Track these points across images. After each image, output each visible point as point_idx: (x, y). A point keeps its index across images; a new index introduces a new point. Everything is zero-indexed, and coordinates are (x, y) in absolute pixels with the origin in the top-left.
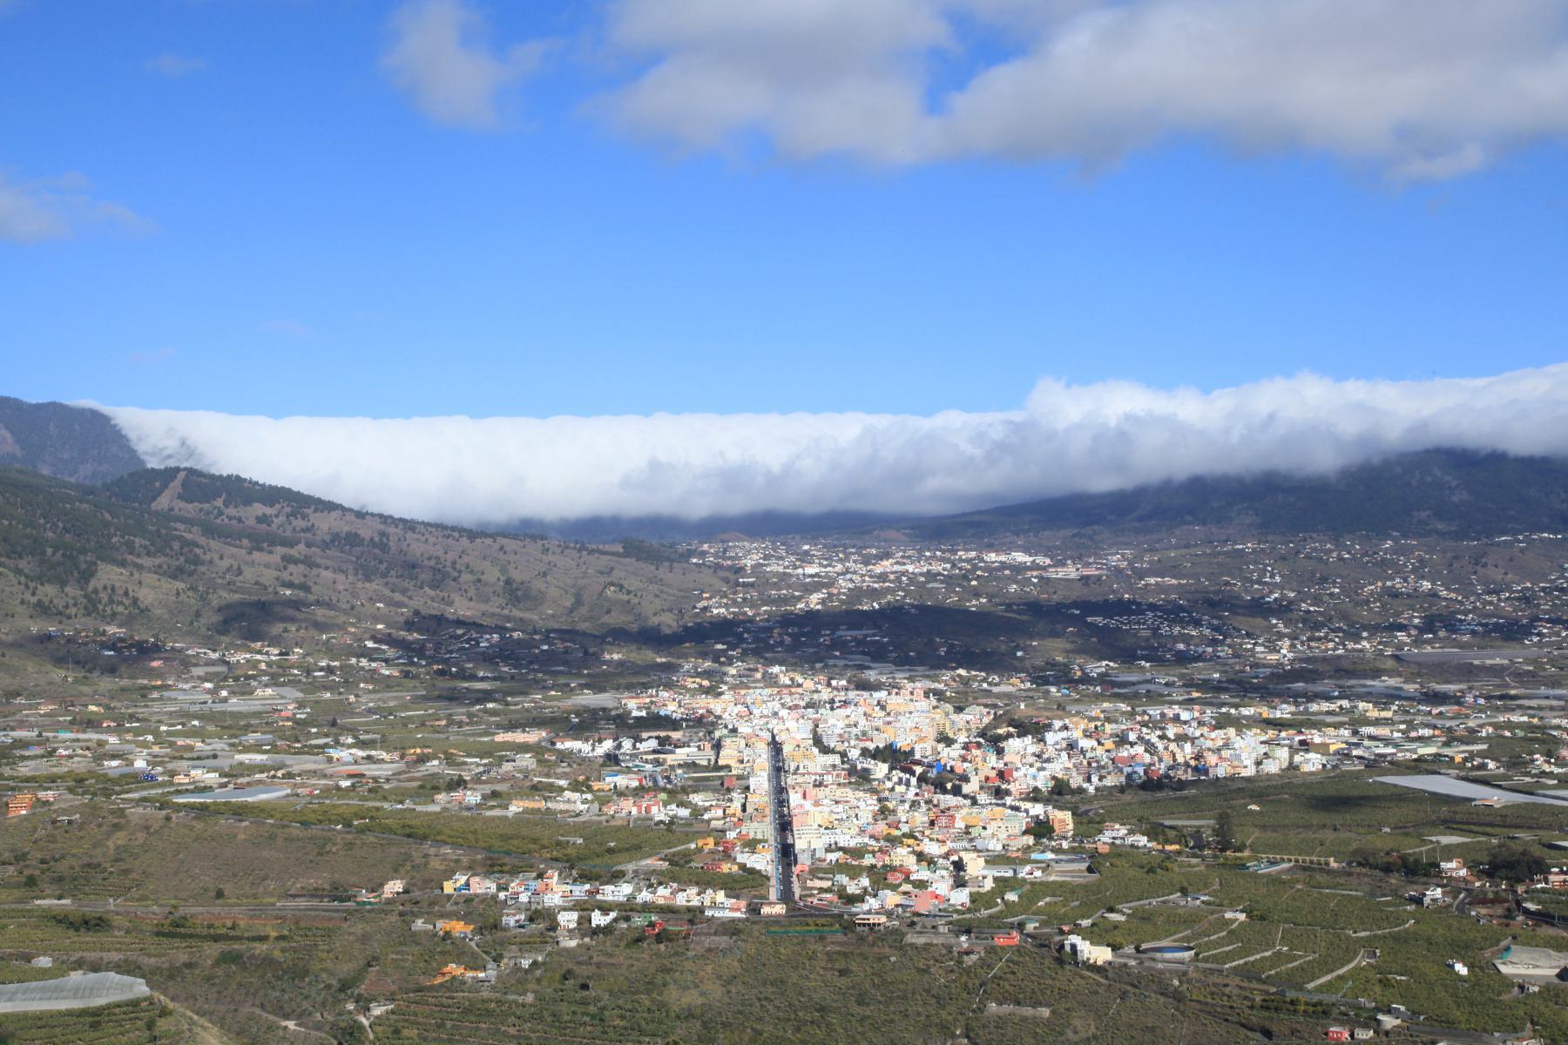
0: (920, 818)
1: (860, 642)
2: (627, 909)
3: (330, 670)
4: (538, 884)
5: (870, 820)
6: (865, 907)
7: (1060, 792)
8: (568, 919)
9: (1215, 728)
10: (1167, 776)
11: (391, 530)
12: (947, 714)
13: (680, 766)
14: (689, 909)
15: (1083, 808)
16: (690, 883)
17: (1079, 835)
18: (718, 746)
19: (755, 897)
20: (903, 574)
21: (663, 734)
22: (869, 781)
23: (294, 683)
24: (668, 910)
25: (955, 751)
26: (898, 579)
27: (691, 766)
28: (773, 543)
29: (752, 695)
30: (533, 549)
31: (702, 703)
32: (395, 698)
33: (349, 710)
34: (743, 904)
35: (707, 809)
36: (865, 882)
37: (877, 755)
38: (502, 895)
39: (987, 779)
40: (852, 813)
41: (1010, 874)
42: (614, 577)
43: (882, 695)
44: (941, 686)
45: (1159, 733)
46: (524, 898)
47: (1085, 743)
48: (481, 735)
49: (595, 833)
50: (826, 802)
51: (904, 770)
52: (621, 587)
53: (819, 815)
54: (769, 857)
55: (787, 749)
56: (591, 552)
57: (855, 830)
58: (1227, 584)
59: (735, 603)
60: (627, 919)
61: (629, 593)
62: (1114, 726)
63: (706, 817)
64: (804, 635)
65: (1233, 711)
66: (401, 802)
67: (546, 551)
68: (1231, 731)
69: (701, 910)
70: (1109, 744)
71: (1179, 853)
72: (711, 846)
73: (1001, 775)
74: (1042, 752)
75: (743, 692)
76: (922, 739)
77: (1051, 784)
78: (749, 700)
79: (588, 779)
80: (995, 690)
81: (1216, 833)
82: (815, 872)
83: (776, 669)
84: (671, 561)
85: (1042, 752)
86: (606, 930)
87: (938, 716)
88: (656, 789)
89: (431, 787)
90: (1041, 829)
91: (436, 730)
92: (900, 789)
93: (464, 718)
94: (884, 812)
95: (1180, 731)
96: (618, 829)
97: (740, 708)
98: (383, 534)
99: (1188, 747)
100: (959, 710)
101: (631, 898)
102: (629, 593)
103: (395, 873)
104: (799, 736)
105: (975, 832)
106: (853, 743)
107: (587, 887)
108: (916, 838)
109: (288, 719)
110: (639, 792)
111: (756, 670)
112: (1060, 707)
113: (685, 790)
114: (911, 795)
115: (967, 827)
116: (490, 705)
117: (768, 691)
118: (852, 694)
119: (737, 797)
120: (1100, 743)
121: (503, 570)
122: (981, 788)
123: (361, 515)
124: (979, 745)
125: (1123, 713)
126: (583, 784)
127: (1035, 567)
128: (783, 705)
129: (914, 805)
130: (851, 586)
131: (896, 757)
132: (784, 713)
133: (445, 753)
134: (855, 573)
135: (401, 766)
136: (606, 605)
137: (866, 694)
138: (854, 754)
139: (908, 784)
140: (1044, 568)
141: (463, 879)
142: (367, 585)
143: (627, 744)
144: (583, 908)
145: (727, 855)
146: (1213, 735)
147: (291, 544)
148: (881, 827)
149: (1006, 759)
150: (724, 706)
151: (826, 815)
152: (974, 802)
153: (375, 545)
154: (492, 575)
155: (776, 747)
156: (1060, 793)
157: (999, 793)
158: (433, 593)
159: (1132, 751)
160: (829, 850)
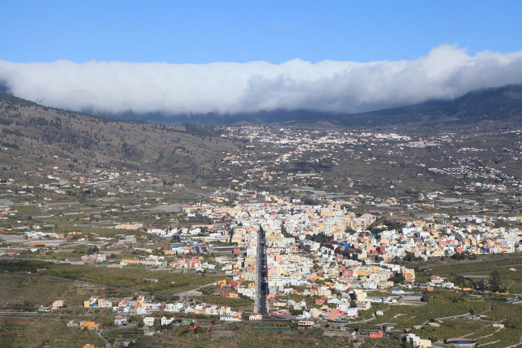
0: (335, 271)
1: (308, 180)
3: (28, 190)
4: (134, 303)
5: (309, 272)
6: (303, 317)
7: (409, 259)
8: (149, 321)
9: (495, 227)
10: (467, 252)
11: (62, 117)
12: (352, 218)
13: (211, 243)
14: (212, 317)
15: (421, 268)
16: (213, 303)
17: (418, 282)
18: (231, 233)
19: (246, 310)
20: (332, 144)
21: (203, 226)
22: (309, 251)
23: (9, 197)
24: (201, 317)
25: (355, 237)
26: (329, 147)
27: (218, 243)
28: (265, 127)
29: (251, 207)
30: (138, 128)
31: (224, 210)
32: (63, 205)
33: (38, 212)
34: (239, 314)
35: (224, 265)
36: (304, 304)
37: (313, 238)
38: (115, 308)
39: (371, 251)
40: (299, 268)
41: (380, 301)
42: (182, 142)
43: (318, 207)
44: (350, 203)
45: (463, 229)
46: (126, 310)
47: (424, 234)
48: (108, 225)
50: (286, 262)
51: (328, 246)
52: (184, 149)
53: (281, 269)
54: (254, 290)
55: (268, 235)
56: (169, 130)
57: (300, 277)
58: (505, 151)
59: (243, 158)
60: (180, 321)
61: (188, 152)
62: (439, 225)
63: (223, 269)
64: (279, 175)
65: (505, 219)
66: (63, 260)
67: (145, 129)
68: (503, 229)
69: (218, 317)
70: (436, 235)
71: (470, 292)
72: (225, 284)
73: (378, 249)
74: (401, 238)
75: (246, 205)
76: (338, 231)
77: (405, 255)
78: (249, 209)
79: (162, 249)
80: (378, 205)
81: (491, 282)
82: (278, 299)
83: (264, 193)
84: (211, 136)
85: (401, 238)
86: (169, 327)
87: (347, 218)
88: (198, 254)
89: (80, 252)
90: (398, 278)
91: (85, 223)
92: (326, 256)
93: (99, 216)
94: (316, 268)
95: (474, 228)
96: (176, 275)
97: (244, 213)
98: (58, 119)
99: (478, 237)
100: (359, 215)
101: (182, 310)
102: (188, 152)
103: (59, 296)
104: (274, 228)
105: (363, 279)
106: (302, 232)
107: (159, 304)
108: (332, 282)
109: (5, 216)
110: (189, 256)
111: (254, 193)
112: (412, 215)
113: (213, 255)
114: (331, 259)
115: (359, 276)
116: (113, 210)
117: (259, 204)
118: (303, 207)
119: (240, 259)
120: (431, 234)
121: (122, 139)
122: (368, 256)
123: (46, 109)
124: (367, 234)
125: (446, 219)
126: (160, 251)
127: (402, 141)
128: (266, 212)
129: (332, 264)
130: (304, 150)
131: (324, 239)
132: (267, 216)
133: (89, 234)
134: (307, 143)
135: (64, 241)
136: (176, 158)
137: (310, 207)
138: (302, 237)
139: (330, 254)
140: (407, 142)
141: (95, 300)
142: (49, 146)
143: (185, 231)
144: (157, 315)
145: (233, 289)
146: (492, 231)
147: (8, 123)
148: (314, 276)
149: (382, 241)
150: (237, 212)
151: (285, 269)
152: (364, 264)
153: (54, 125)
154: (116, 141)
155: (262, 233)
156: (409, 260)
157: (377, 259)
158: (84, 151)
159: (449, 239)
160: (285, 287)
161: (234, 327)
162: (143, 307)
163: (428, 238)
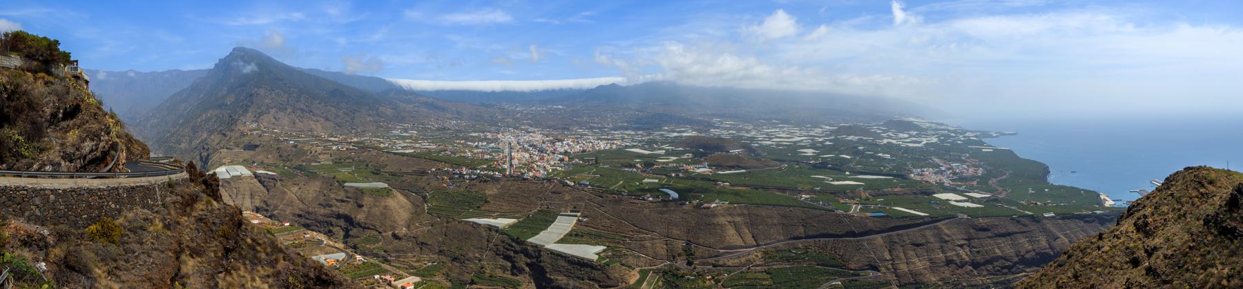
2: (479, 176)
7: (566, 153)
49: (472, 160)
90: (562, 160)
131: (534, 146)
161: (498, 180)
162: (464, 171)
163: (570, 145)
